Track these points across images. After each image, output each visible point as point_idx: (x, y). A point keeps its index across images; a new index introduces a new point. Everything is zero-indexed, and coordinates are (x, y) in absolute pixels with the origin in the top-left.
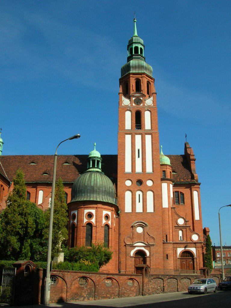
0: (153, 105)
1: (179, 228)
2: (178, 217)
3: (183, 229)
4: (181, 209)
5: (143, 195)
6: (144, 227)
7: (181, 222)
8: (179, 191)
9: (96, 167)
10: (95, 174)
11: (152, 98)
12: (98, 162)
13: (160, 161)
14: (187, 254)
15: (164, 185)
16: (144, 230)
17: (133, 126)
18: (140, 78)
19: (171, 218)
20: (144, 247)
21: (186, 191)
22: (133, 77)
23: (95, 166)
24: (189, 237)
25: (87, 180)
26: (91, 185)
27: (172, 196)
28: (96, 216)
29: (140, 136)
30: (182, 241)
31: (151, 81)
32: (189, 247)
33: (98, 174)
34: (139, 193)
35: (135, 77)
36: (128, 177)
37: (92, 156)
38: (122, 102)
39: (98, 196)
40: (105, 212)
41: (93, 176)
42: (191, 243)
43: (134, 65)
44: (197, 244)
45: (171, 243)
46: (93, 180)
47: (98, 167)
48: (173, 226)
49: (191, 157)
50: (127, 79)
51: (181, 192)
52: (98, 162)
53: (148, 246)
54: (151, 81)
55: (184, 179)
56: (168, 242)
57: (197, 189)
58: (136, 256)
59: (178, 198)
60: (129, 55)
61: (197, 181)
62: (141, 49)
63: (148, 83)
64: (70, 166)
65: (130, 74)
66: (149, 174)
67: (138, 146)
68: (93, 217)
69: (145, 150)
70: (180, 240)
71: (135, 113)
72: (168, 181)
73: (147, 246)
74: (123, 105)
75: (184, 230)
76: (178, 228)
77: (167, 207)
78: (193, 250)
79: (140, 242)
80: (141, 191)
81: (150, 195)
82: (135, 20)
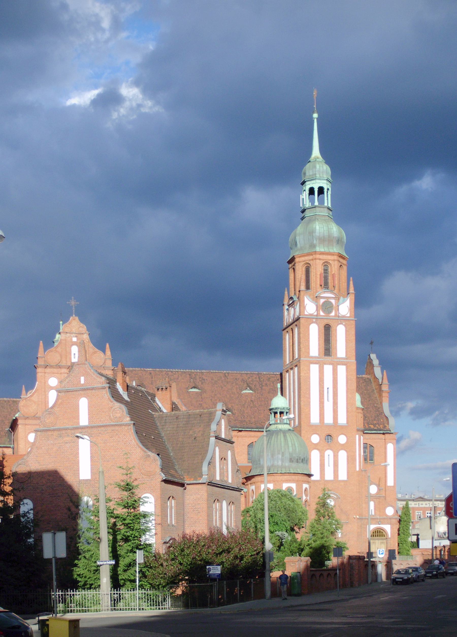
3: (375, 500)
5: (334, 456)
18: (331, 262)
22: (320, 259)
30: (373, 516)
34: (329, 453)
35: (323, 260)
36: (315, 429)
42: (384, 518)
46: (290, 444)
50: (310, 260)
55: (374, 425)
64: (201, 394)
66: (342, 427)
70: (371, 514)
78: (387, 528)
80: (331, 449)
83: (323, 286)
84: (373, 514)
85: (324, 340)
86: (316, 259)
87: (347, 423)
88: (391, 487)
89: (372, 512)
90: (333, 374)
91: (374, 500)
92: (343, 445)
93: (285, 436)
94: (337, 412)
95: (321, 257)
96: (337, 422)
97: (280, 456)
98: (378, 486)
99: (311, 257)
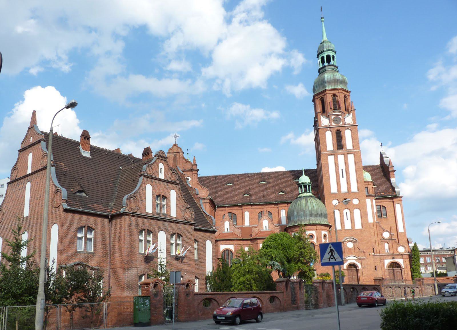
0: (352, 123)
1: (385, 241)
2: (383, 231)
4: (384, 223)
5: (350, 213)
6: (354, 242)
7: (386, 235)
8: (380, 205)
9: (308, 191)
10: (310, 198)
11: (351, 115)
12: (309, 186)
13: (363, 180)
14: (395, 265)
15: (368, 201)
16: (354, 245)
17: (334, 147)
19: (376, 233)
20: (356, 260)
21: (387, 203)
22: (329, 94)
23: (307, 191)
24: (395, 249)
25: (304, 206)
26: (309, 210)
27: (375, 211)
28: (317, 236)
29: (343, 156)
30: (389, 253)
31: (347, 95)
32: (396, 259)
33: (312, 199)
34: (346, 211)
36: (335, 196)
37: (303, 181)
38: (321, 122)
39: (316, 219)
40: (323, 233)
41: (309, 202)
42: (397, 255)
43: (329, 80)
44: (403, 256)
45: (378, 255)
46: (309, 205)
47: (309, 192)
48: (379, 240)
49: (390, 170)
50: (323, 96)
51: (382, 206)
52: (309, 186)
53: (359, 259)
54: (347, 95)
55: (385, 193)
56: (378, 254)
57: (399, 202)
58: (348, 268)
59: (382, 213)
60: (321, 66)
61: (399, 193)
62: (333, 57)
63: (345, 97)
65: (325, 90)
66: (355, 193)
67: (342, 165)
68: (314, 238)
69: (349, 170)
70: (386, 252)
71: (335, 133)
72: (371, 197)
73: (359, 259)
74: (322, 125)
75: (390, 243)
76: (384, 241)
77: (372, 222)
78: (401, 261)
79: (352, 256)
80: (348, 209)
81: (357, 213)
82: (323, 19)
83: (333, 108)
84: (388, 252)
85: (336, 140)
86: (326, 94)
87: (358, 190)
88: (402, 233)
89: (387, 251)
90: (345, 160)
91: (387, 242)
92: (356, 205)
93: (306, 200)
94: (350, 184)
95: (330, 92)
96: (351, 191)
97: (303, 213)
98: (390, 233)
99: (323, 94)
